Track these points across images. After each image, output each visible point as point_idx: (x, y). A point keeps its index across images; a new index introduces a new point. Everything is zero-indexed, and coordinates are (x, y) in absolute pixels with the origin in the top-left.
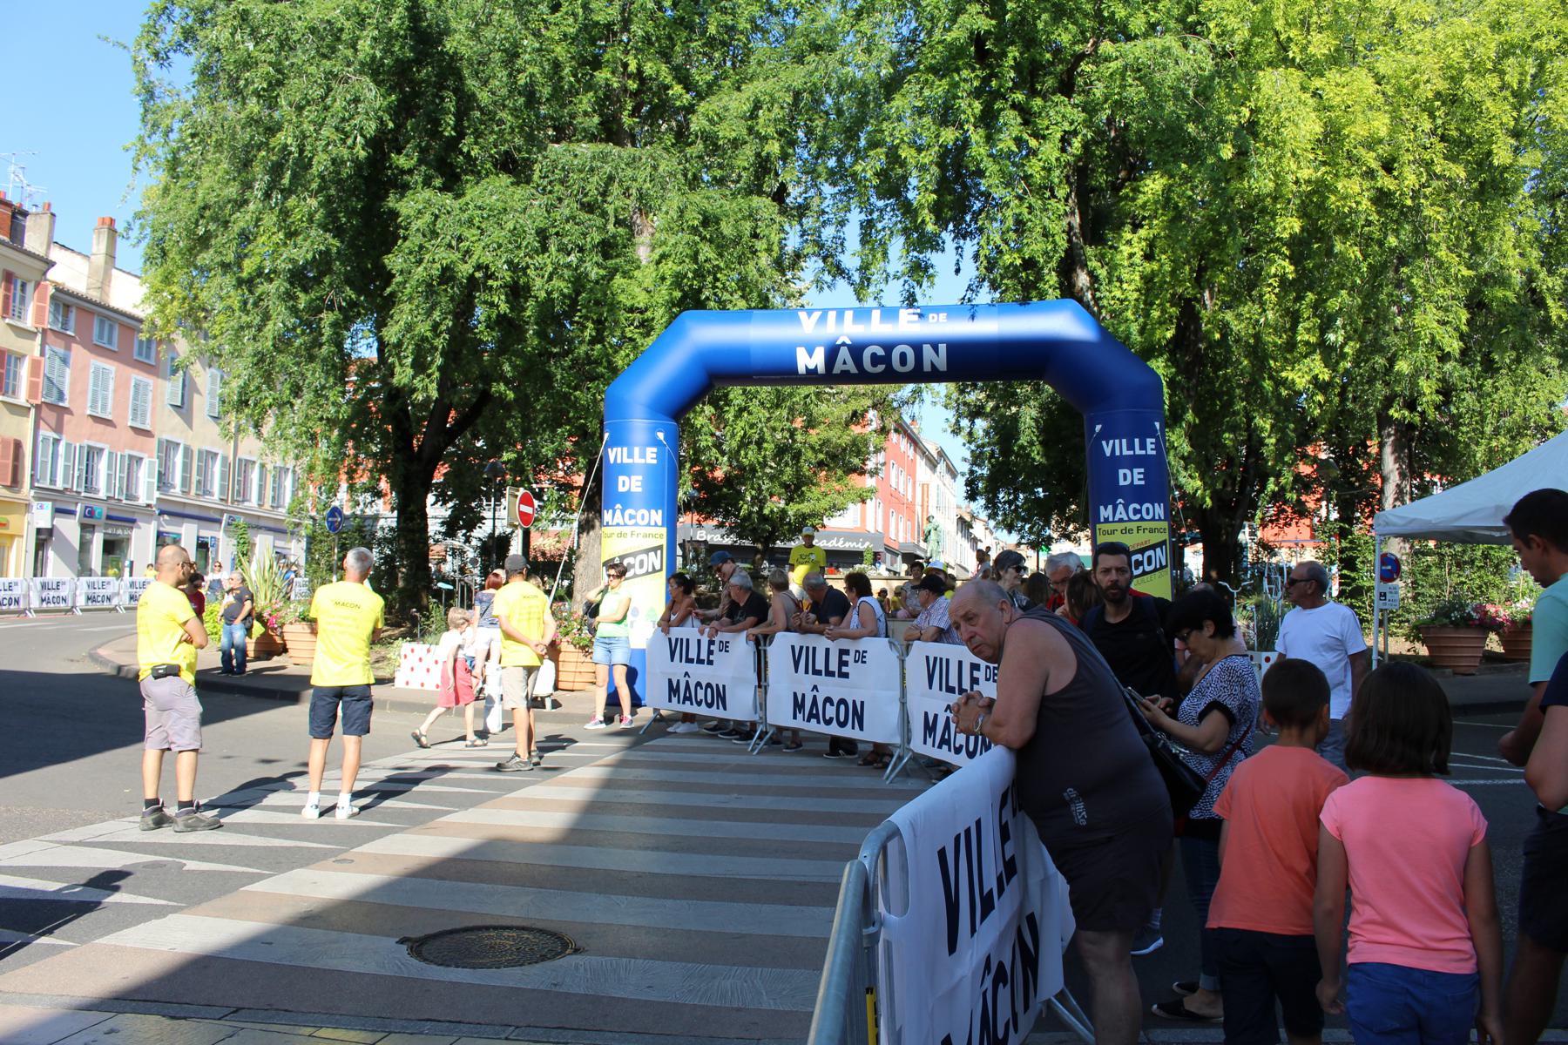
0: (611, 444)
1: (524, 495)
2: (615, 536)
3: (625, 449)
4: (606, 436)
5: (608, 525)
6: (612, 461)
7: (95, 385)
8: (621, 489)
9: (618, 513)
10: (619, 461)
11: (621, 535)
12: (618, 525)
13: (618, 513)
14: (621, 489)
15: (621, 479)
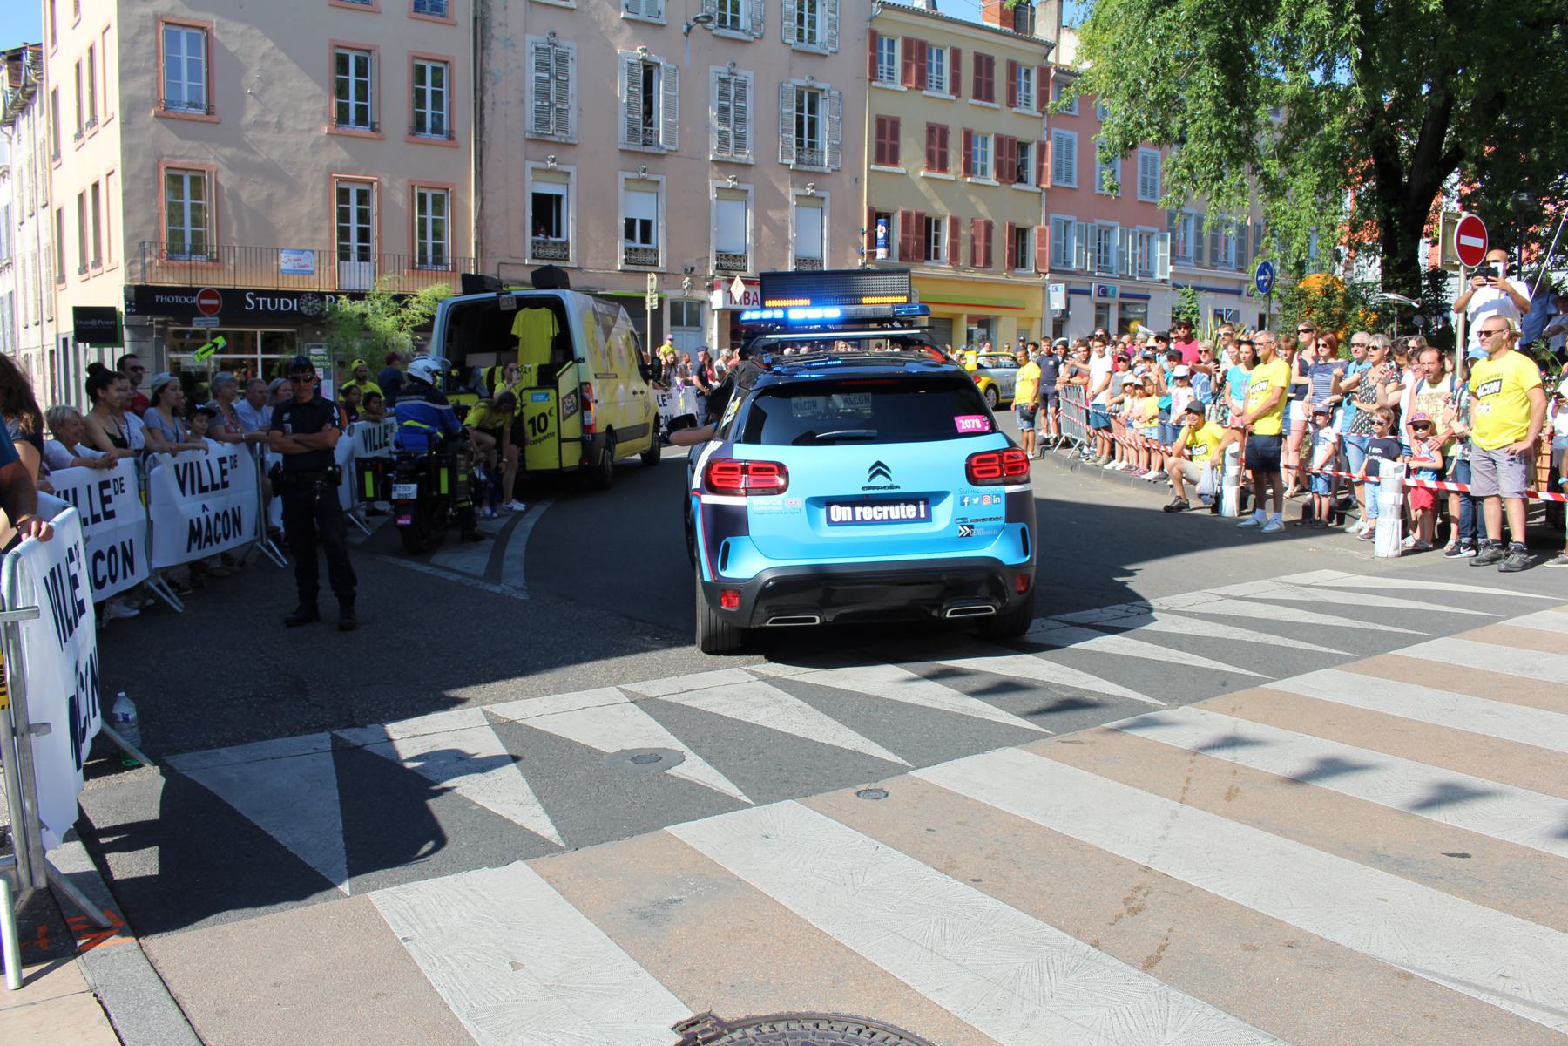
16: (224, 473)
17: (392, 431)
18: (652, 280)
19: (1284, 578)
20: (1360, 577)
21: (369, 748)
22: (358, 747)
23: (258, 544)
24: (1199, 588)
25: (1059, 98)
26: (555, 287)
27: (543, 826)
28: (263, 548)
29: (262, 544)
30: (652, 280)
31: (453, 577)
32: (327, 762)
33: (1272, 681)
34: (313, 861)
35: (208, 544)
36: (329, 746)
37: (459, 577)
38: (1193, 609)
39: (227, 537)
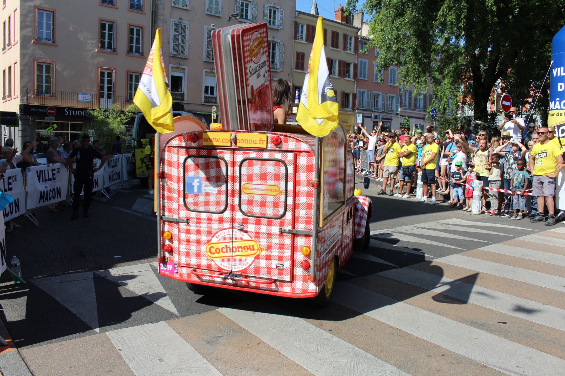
0: (555, 66)
1: (505, 96)
2: (555, 115)
3: (562, 68)
4: (552, 62)
5: (552, 109)
6: (555, 76)
7: (391, 75)
8: (559, 90)
9: (557, 103)
10: (559, 75)
11: (559, 114)
12: (557, 109)
13: (557, 103)
14: (559, 90)
15: (559, 84)
16: (54, 174)
17: (118, 161)
18: (214, 108)
19: (440, 221)
20: (466, 221)
21: (107, 278)
22: (104, 277)
23: (68, 201)
24: (410, 224)
25: (362, 49)
26: (179, 111)
27: (173, 310)
28: (69, 202)
29: (69, 201)
30: (214, 108)
31: (139, 215)
32: (92, 283)
33: (436, 258)
34: (86, 320)
35: (46, 200)
36: (92, 277)
37: (142, 215)
38: (407, 232)
39: (54, 198)
